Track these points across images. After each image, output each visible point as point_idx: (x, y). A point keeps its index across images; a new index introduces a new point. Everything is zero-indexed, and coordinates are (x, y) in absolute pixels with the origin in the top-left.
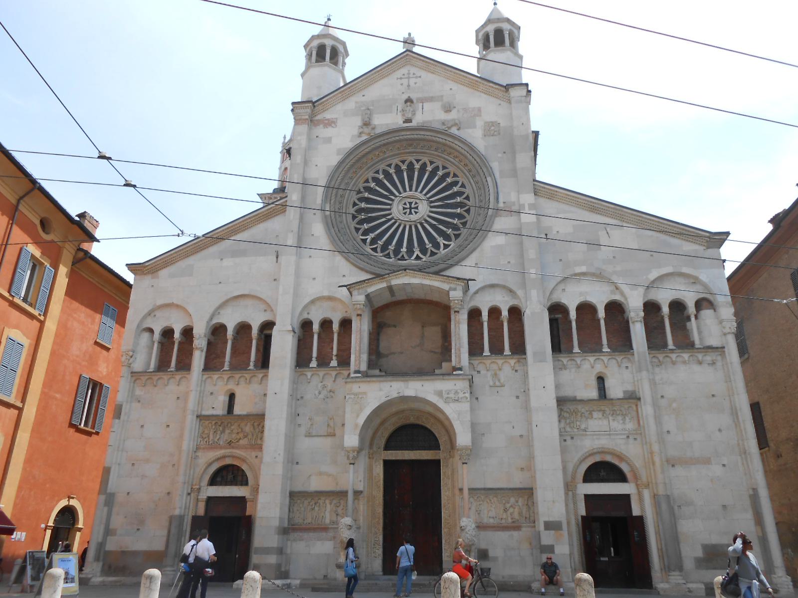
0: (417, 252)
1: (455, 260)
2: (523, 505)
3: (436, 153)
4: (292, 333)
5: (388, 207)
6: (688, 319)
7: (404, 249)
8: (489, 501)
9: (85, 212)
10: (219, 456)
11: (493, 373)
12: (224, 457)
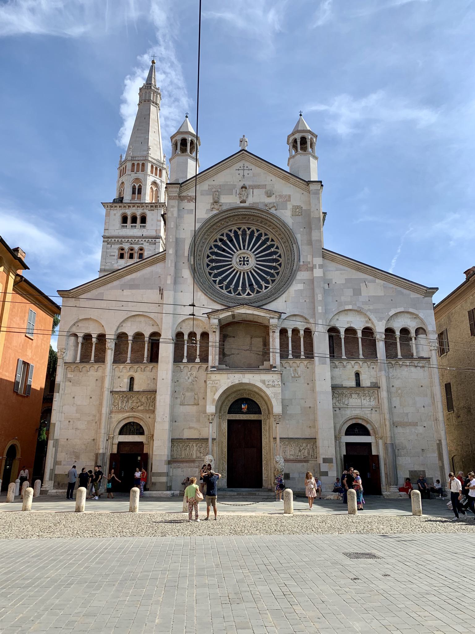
0: (248, 290)
1: (274, 296)
2: (310, 448)
3: (261, 225)
5: (230, 259)
6: (411, 339)
7: (240, 288)
9: (18, 248)
10: (126, 417)
11: (294, 369)
12: (129, 417)
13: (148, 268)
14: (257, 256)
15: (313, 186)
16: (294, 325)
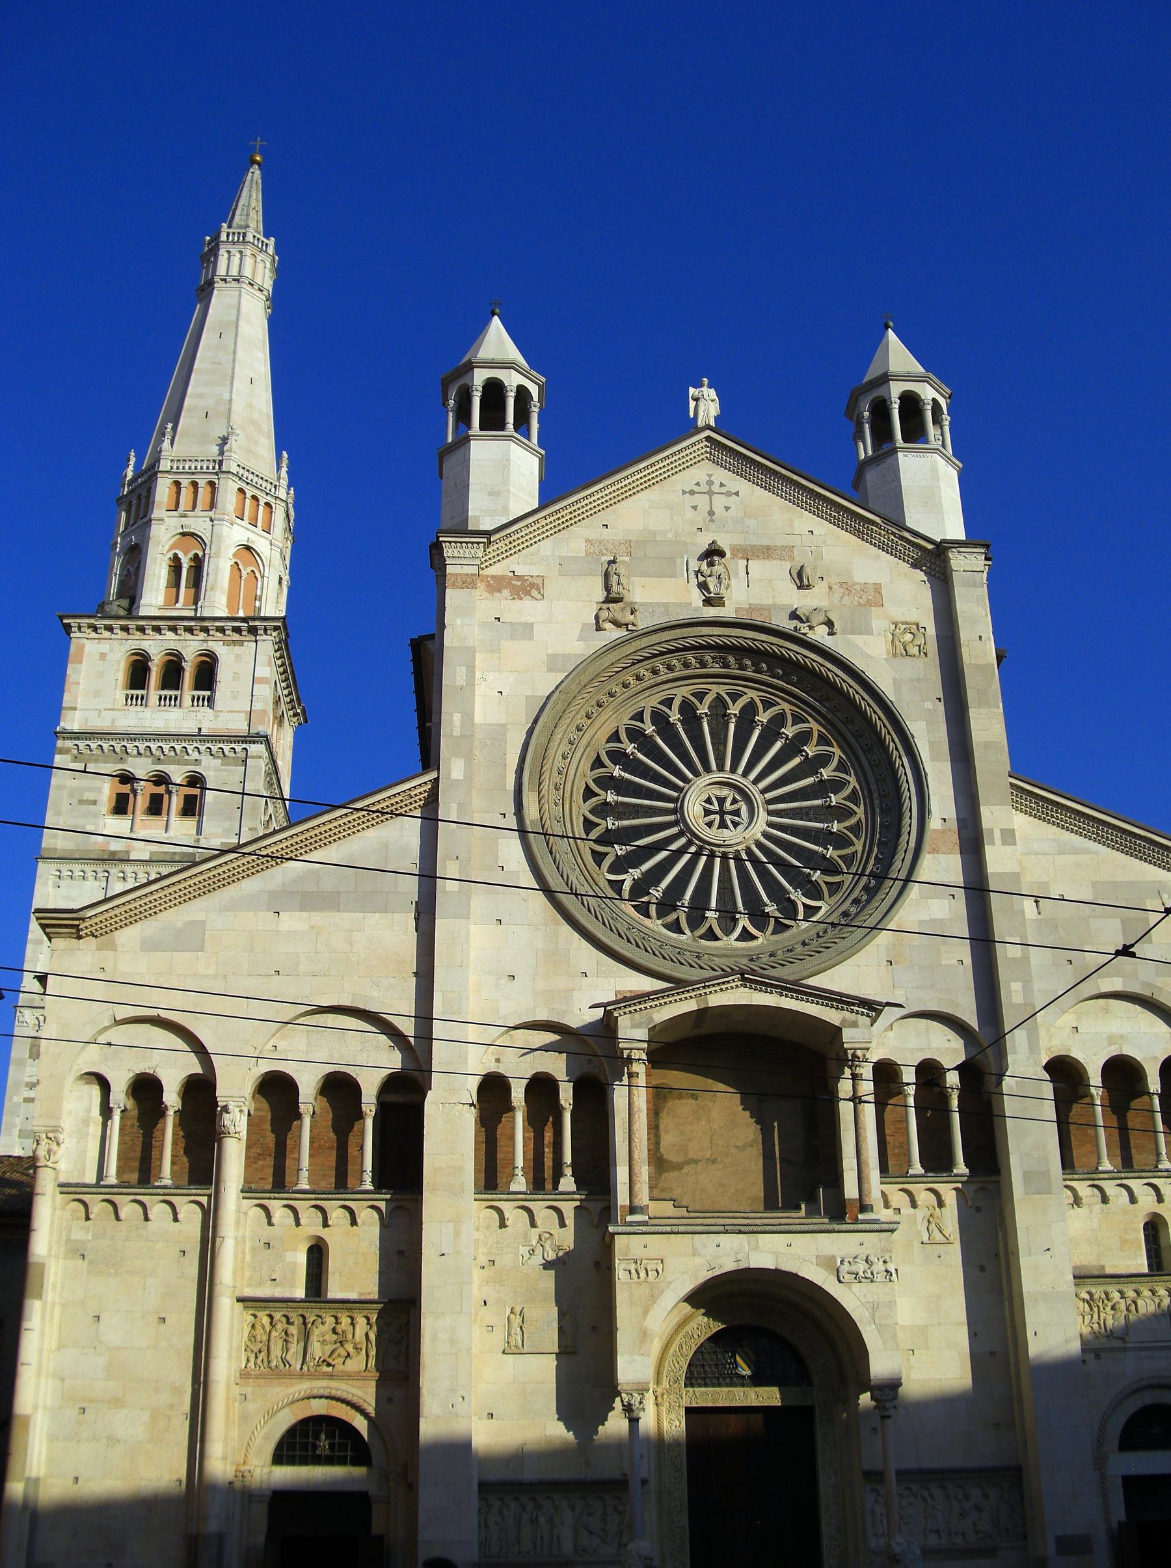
0: (744, 922)
8: (926, 1494)
13: (372, 829)
14: (769, 795)
16: (921, 1050)
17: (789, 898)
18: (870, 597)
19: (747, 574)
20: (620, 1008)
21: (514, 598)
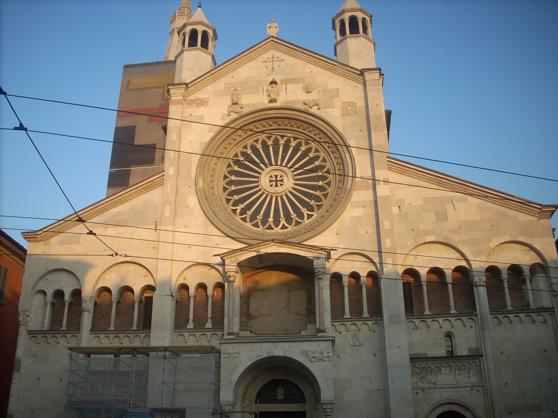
0: (283, 222)
4: (171, 297)
5: (256, 180)
6: (524, 281)
7: (271, 219)
13: (141, 196)
14: (295, 173)
15: (369, 75)
17: (302, 212)
18: (334, 94)
19: (286, 89)
20: (225, 256)
21: (197, 107)
